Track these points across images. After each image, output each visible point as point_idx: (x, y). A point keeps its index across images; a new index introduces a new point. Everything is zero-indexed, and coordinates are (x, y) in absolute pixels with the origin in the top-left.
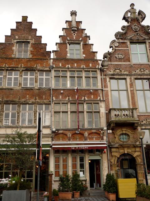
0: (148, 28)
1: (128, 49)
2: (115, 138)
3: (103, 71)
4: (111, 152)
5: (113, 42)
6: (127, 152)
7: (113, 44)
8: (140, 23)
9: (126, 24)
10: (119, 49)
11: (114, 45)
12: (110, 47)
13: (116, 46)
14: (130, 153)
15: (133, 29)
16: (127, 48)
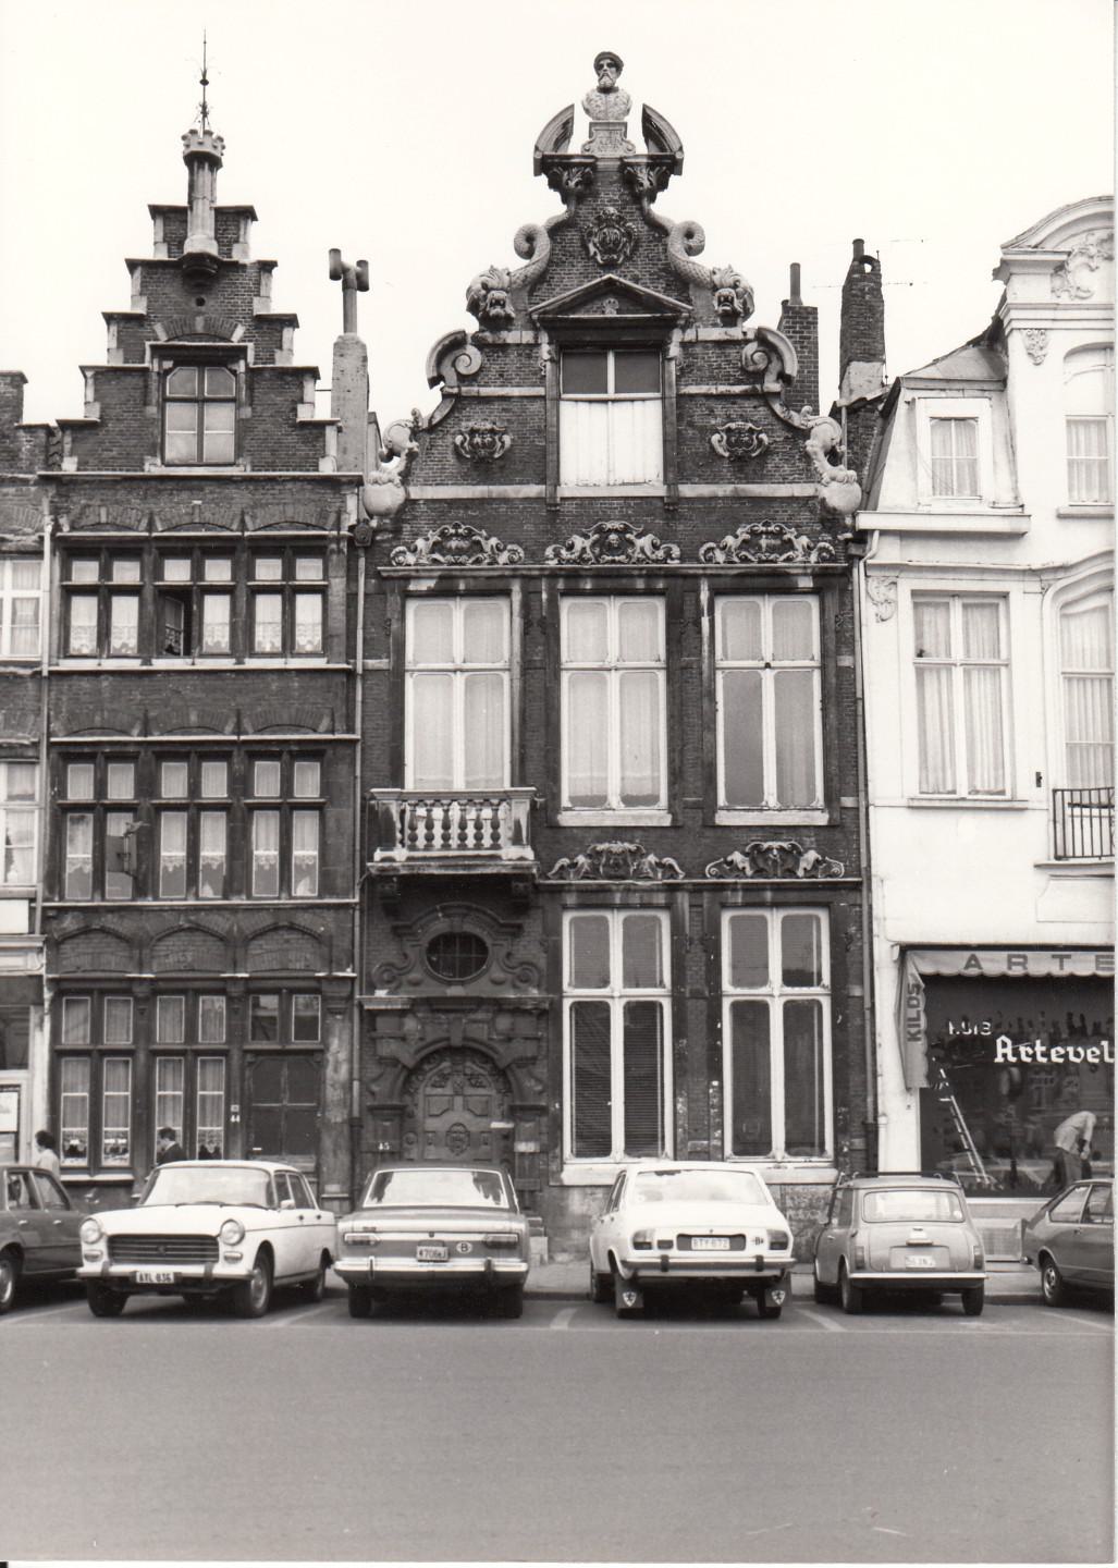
0: (692, 243)
1: (540, 391)
2: (406, 956)
3: (366, 549)
4: (374, 1040)
5: (452, 346)
6: (465, 1039)
7: (447, 362)
8: (645, 203)
9: (548, 206)
10: (485, 391)
11: (453, 365)
12: (433, 382)
13: (463, 370)
14: (483, 1049)
15: (592, 249)
16: (534, 385)
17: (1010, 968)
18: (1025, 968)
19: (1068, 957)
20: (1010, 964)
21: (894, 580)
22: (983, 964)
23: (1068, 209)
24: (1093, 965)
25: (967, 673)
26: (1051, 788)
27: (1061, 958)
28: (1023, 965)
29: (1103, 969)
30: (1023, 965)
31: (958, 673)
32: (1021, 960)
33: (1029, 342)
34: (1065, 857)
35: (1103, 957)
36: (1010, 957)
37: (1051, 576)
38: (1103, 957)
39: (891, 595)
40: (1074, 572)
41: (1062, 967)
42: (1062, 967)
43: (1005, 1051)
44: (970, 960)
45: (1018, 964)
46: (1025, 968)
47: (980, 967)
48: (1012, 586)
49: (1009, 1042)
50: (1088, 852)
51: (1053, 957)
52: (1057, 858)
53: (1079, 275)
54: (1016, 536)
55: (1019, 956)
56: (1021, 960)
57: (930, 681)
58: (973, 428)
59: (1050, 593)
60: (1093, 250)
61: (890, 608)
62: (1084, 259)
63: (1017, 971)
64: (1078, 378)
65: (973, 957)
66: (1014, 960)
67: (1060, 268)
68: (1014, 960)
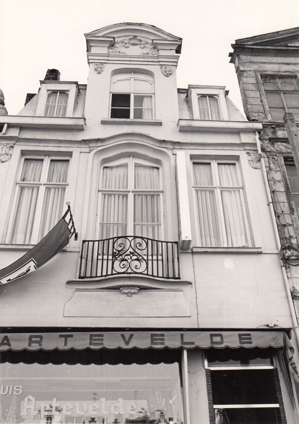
17: (30, 345)
18: (40, 345)
19: (71, 336)
20: (31, 342)
21: (13, 145)
22: (12, 343)
23: (115, 25)
24: (88, 341)
25: (48, 189)
26: (82, 239)
27: (66, 337)
28: (39, 343)
29: (95, 344)
30: (39, 343)
31: (42, 189)
32: (38, 339)
33: (95, 66)
34: (85, 277)
35: (95, 335)
36: (31, 337)
37: (94, 145)
38: (95, 335)
39: (10, 152)
40: (106, 143)
41: (66, 344)
42: (66, 344)
43: (29, 407)
44: (3, 340)
45: (36, 342)
46: (40, 345)
47: (9, 345)
48: (76, 151)
49: (33, 399)
50: (99, 274)
51: (61, 336)
52: (80, 277)
53: (120, 48)
54: (80, 129)
55: (37, 337)
56: (38, 339)
57: (27, 193)
58: (68, 95)
59: (94, 152)
60: (126, 41)
61: (7, 157)
62: (123, 44)
63: (35, 347)
64: (119, 82)
65: (6, 338)
66: (33, 339)
67: (112, 45)
68: (33, 339)
